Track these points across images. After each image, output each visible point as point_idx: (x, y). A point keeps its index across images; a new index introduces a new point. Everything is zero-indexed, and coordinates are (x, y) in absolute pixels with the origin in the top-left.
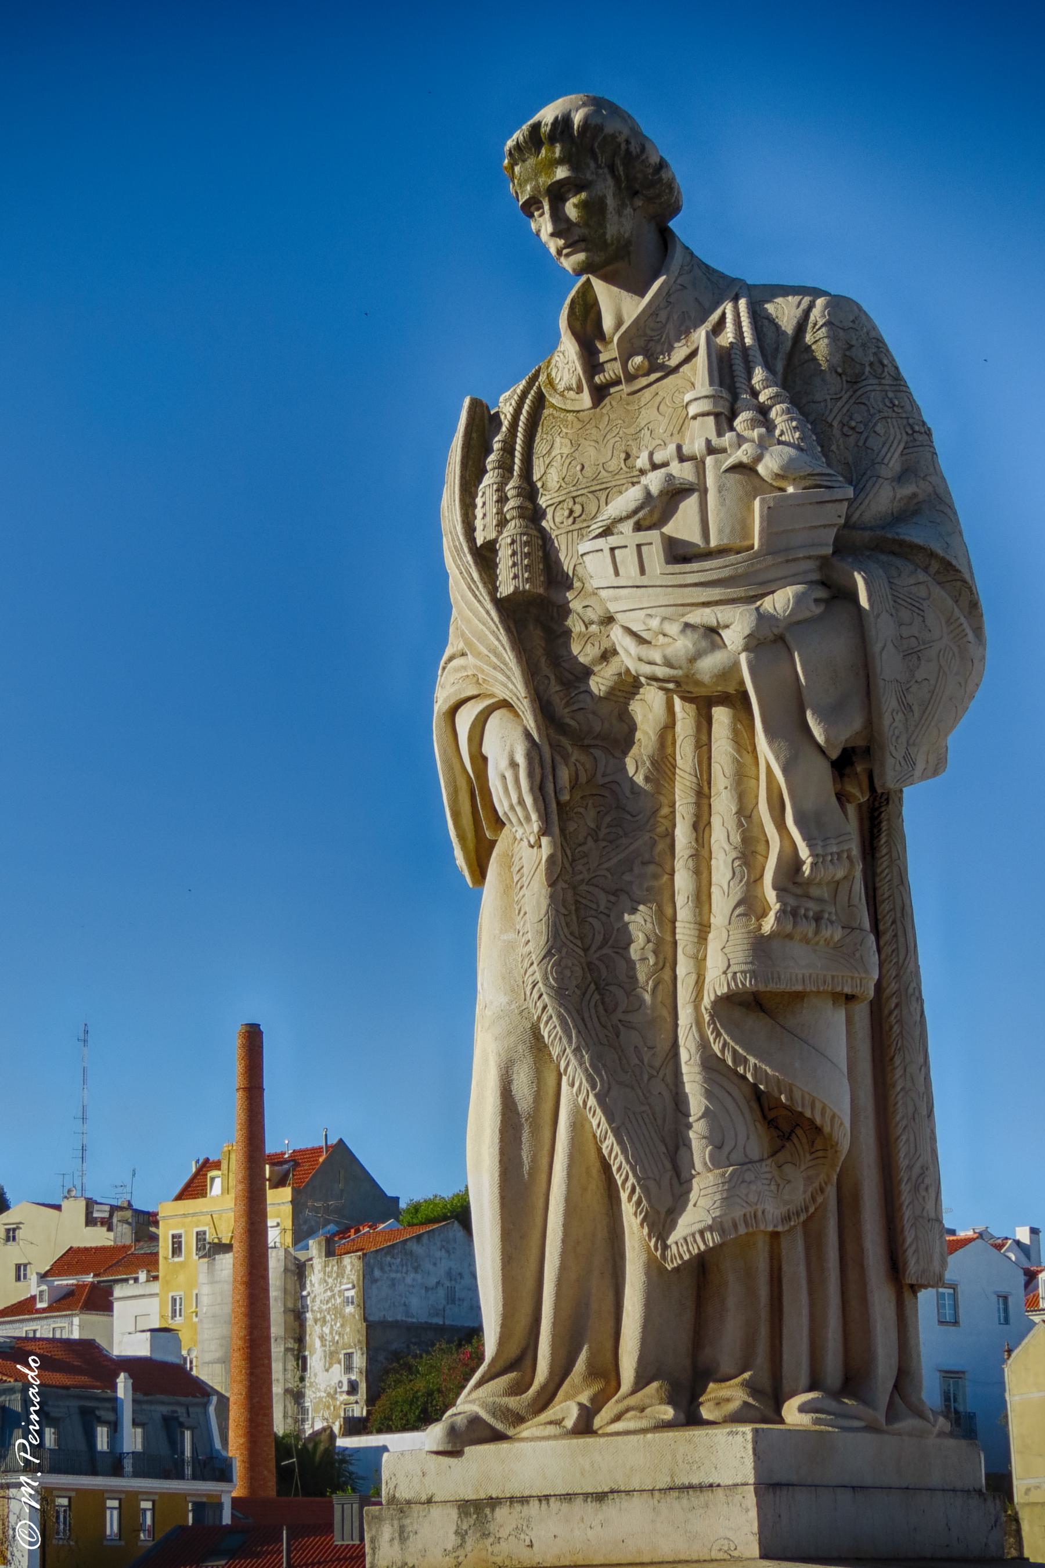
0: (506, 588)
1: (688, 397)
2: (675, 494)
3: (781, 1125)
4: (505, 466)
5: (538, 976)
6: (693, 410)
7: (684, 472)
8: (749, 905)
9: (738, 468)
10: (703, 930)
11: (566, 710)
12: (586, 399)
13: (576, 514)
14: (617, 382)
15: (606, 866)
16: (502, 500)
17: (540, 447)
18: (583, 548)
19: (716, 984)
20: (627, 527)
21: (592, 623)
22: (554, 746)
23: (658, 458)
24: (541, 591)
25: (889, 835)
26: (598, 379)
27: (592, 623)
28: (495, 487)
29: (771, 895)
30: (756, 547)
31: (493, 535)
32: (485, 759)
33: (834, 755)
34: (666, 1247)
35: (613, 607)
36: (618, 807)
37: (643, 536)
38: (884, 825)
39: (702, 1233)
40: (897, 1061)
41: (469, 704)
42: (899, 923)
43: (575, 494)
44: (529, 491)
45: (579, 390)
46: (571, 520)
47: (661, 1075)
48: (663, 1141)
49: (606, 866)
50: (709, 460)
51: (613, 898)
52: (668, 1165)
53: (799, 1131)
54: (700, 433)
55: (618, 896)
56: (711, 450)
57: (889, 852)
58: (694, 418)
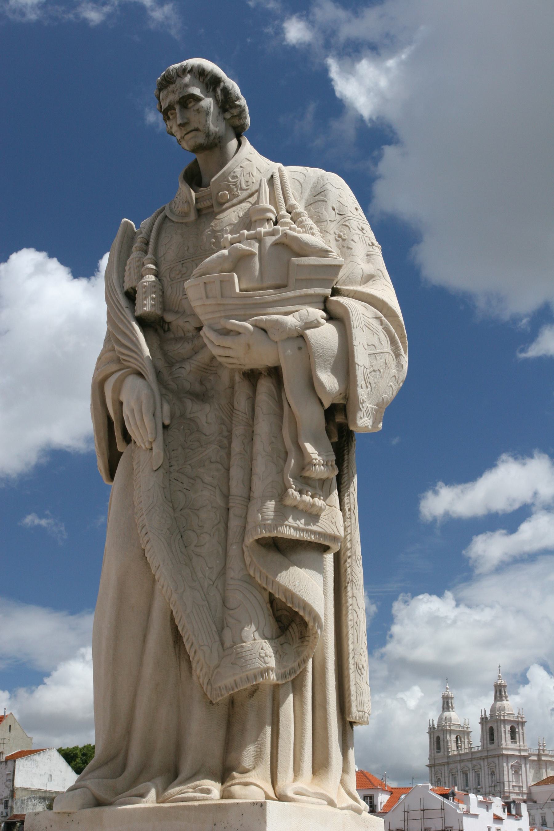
11: (170, 377)
13: (183, 273)
15: (190, 462)
25: (348, 463)
28: (137, 259)
31: (133, 285)
36: (197, 431)
40: (349, 589)
42: (352, 512)
43: (182, 262)
46: (180, 276)
47: (215, 584)
48: (215, 623)
49: (190, 462)
51: (191, 481)
52: (217, 638)
53: (294, 625)
55: (195, 480)
57: (348, 472)
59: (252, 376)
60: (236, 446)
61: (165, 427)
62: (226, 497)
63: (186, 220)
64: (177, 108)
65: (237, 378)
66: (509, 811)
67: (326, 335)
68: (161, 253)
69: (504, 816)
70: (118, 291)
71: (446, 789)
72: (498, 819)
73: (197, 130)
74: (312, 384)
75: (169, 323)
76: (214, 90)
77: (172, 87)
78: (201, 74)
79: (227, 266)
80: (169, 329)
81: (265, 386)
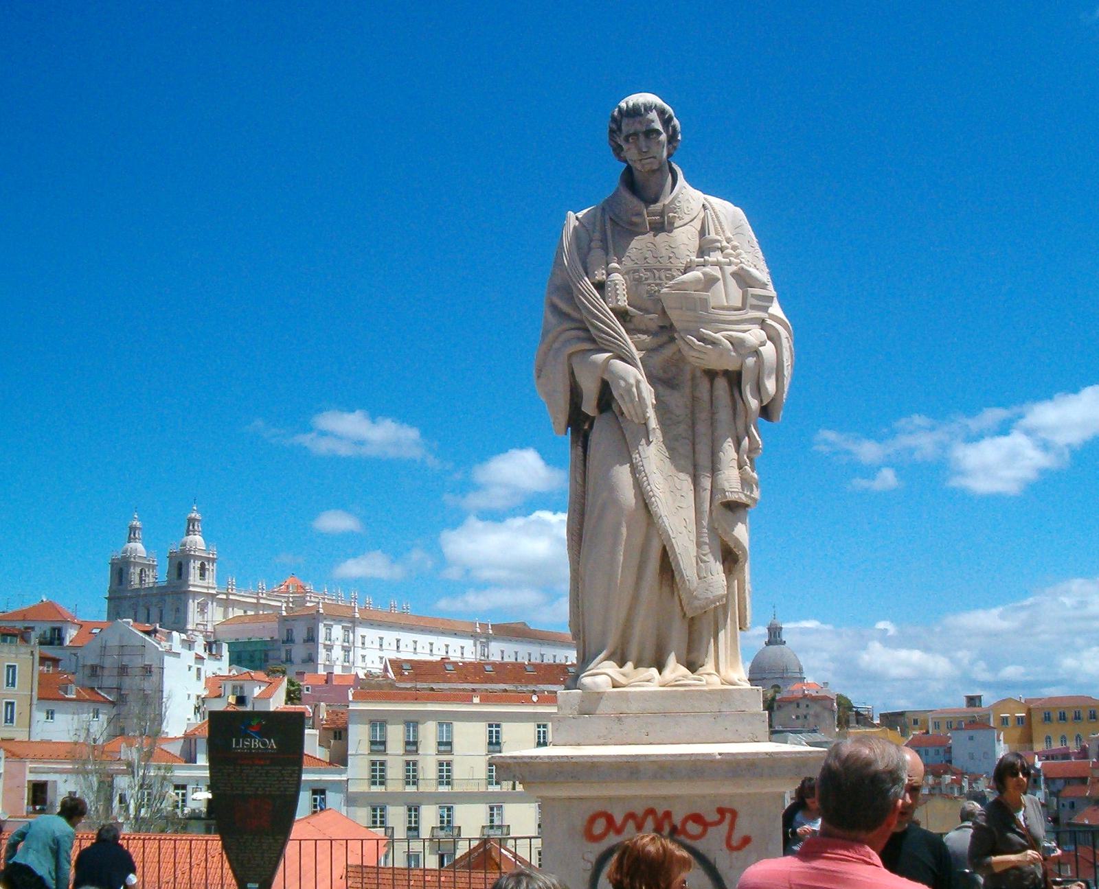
33: (764, 404)
59: (711, 375)
60: (702, 428)
64: (642, 138)
65: (698, 374)
66: (210, 650)
67: (768, 350)
69: (206, 656)
71: (148, 627)
72: (199, 658)
73: (654, 157)
74: (759, 389)
76: (668, 127)
78: (662, 112)
79: (700, 287)
80: (630, 321)
81: (721, 384)
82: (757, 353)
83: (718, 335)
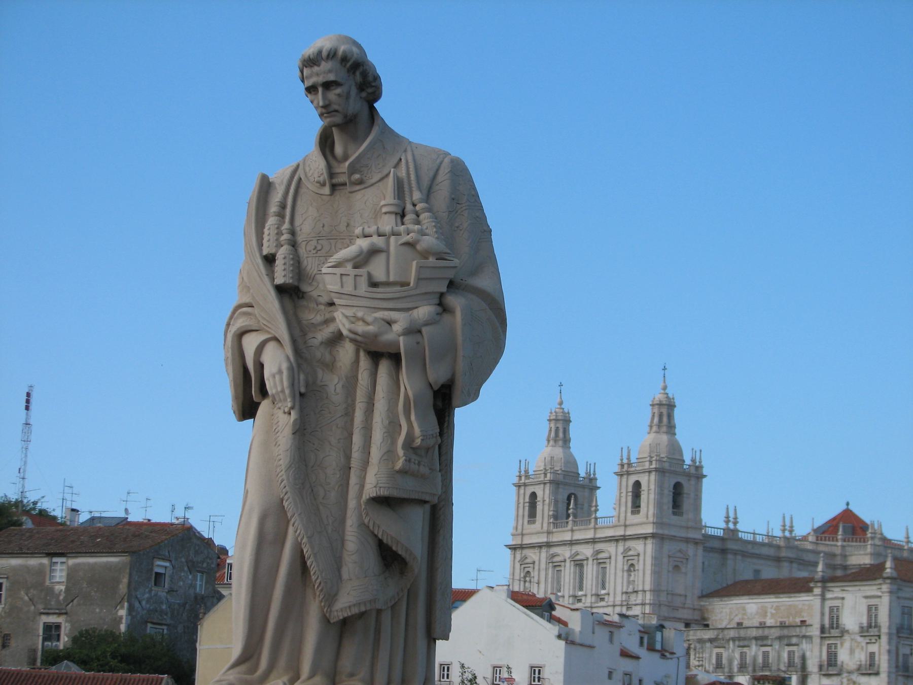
0: (279, 280)
1: (383, 203)
2: (374, 252)
3: (389, 558)
4: (281, 215)
5: (284, 477)
6: (384, 210)
7: (379, 241)
8: (390, 454)
9: (407, 244)
10: (366, 463)
12: (327, 190)
14: (345, 184)
16: (280, 234)
17: (300, 209)
18: (324, 270)
19: (370, 490)
20: (349, 266)
21: (321, 304)
22: (299, 366)
23: (368, 230)
24: (296, 284)
26: (335, 181)
27: (321, 304)
29: (401, 452)
30: (412, 284)
31: (273, 251)
32: (262, 366)
33: (436, 388)
34: (331, 611)
35: (336, 301)
37: (358, 271)
38: (447, 419)
39: (350, 607)
40: (441, 532)
41: (253, 334)
44: (293, 233)
45: (323, 185)
50: (393, 238)
54: (388, 223)
56: (394, 234)
58: (386, 213)
61: (301, 395)
62: (348, 457)
63: (322, 192)
64: (320, 90)
68: (298, 222)
70: (258, 255)
72: (625, 654)
75: (304, 293)
77: (316, 69)
80: (303, 297)
82: (420, 332)
83: (369, 319)
